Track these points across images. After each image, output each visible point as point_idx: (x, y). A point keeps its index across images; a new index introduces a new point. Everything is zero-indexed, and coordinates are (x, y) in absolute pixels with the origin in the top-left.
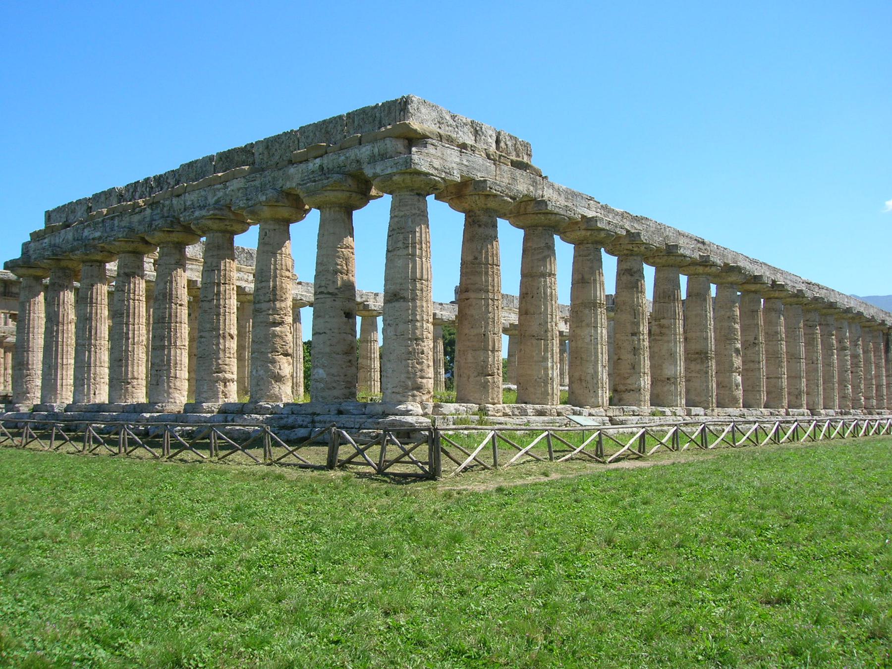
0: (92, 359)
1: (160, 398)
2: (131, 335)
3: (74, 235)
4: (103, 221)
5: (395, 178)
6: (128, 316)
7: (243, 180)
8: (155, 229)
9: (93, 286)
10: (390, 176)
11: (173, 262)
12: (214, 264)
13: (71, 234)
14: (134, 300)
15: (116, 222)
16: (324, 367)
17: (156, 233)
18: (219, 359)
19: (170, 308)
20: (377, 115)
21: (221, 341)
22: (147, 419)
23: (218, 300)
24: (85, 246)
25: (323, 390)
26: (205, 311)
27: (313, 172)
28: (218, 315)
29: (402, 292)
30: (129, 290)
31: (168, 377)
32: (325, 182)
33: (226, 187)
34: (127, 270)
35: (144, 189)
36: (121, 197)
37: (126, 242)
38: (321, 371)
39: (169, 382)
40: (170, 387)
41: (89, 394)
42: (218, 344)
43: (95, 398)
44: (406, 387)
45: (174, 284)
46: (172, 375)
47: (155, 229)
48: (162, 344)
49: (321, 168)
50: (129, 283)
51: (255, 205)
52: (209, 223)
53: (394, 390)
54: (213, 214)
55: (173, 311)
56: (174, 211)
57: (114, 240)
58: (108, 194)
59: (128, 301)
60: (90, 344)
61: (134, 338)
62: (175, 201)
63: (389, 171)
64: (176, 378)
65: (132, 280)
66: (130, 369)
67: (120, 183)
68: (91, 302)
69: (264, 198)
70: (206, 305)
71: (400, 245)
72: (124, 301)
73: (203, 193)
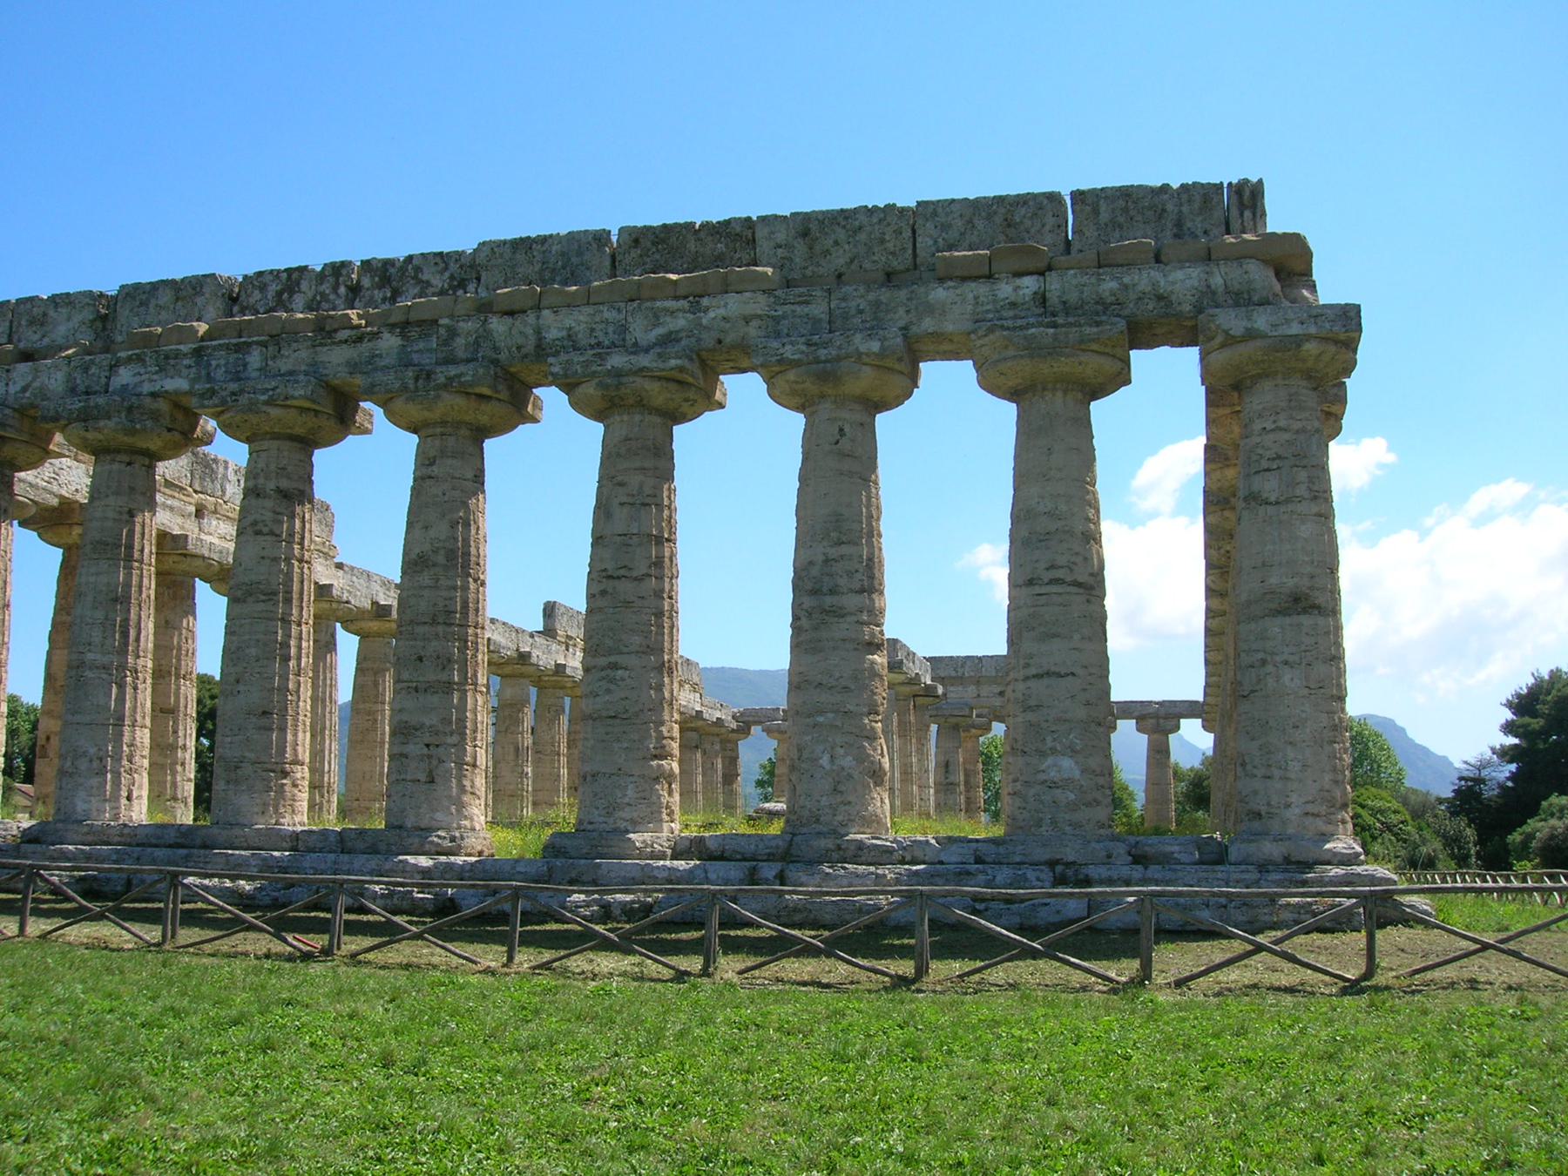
0: (128, 705)
1: (439, 816)
2: (293, 651)
3: (70, 378)
4: (198, 353)
5: (1307, 346)
6: (288, 601)
7: (762, 298)
8: (445, 387)
9: (131, 514)
10: (1298, 341)
11: (470, 475)
12: (647, 490)
13: (60, 376)
14: (301, 561)
15: (255, 359)
16: (1073, 752)
17: (444, 394)
18: (662, 723)
19: (465, 588)
20: (1170, 207)
21: (666, 680)
22: (425, 872)
23: (660, 578)
24: (130, 410)
25: (1073, 807)
26: (627, 604)
27: (1013, 305)
28: (659, 614)
29: (1317, 593)
30: (291, 534)
31: (460, 764)
32: (1088, 330)
33: (696, 308)
34: (285, 484)
35: (326, 288)
36: (234, 296)
37: (302, 410)
38: (1067, 763)
39: (460, 777)
40: (462, 789)
41: (115, 797)
42: (660, 687)
43: (129, 808)
44: (1331, 803)
45: (473, 532)
46: (468, 759)
47: (445, 387)
48: (444, 677)
49: (1041, 299)
50: (292, 516)
51: (839, 359)
52: (653, 387)
53: (1310, 808)
54: (681, 369)
55: (471, 596)
56: (496, 349)
57: (267, 403)
58: (189, 290)
59: (288, 560)
60: (123, 667)
61: (299, 659)
62: (497, 325)
63: (1295, 329)
64: (474, 766)
65: (298, 509)
66: (289, 737)
67: (235, 265)
68: (129, 558)
69: (875, 346)
70: (625, 588)
71: (1301, 491)
72: (276, 560)
73: (610, 315)
